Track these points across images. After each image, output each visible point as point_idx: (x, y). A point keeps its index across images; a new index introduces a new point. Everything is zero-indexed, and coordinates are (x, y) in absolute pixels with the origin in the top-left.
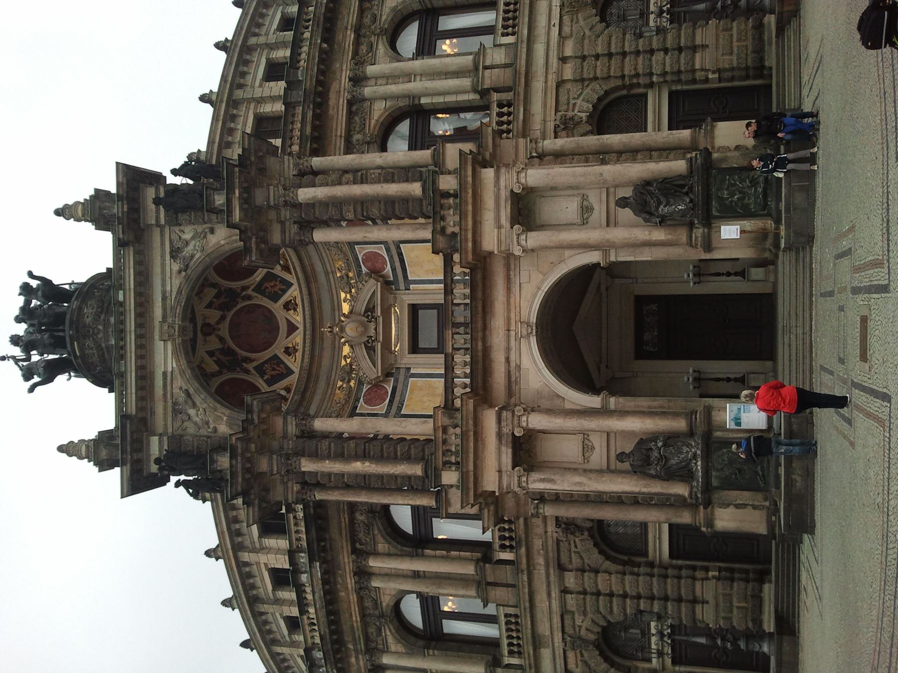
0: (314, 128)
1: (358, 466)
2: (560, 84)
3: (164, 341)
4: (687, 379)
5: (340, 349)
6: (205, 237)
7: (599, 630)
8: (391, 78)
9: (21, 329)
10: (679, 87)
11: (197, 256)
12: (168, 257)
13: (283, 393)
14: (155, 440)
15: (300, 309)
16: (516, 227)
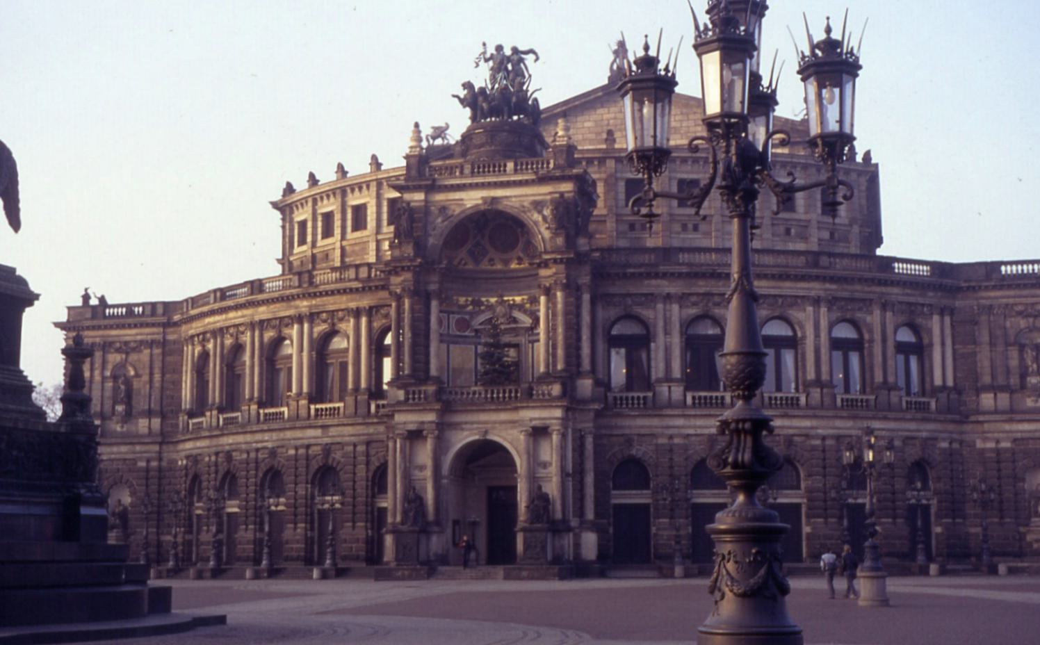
0: (633, 274)
4: (473, 517)
5: (493, 297)
7: (335, 465)
9: (508, 52)
10: (652, 510)
12: (532, 198)
13: (463, 262)
14: (419, 197)
15: (517, 266)
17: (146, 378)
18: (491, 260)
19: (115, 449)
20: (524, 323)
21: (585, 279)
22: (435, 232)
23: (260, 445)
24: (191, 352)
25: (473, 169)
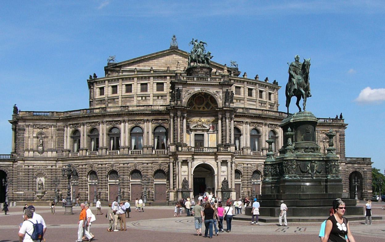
1: (179, 130)
2: (243, 164)
3: (201, 89)
6: (220, 98)
7: (139, 169)
8: (246, 129)
11: (217, 96)
15: (203, 110)
16: (222, 161)
17: (50, 138)
18: (195, 107)
19: (39, 162)
20: (206, 128)
21: (233, 116)
22: (185, 98)
23: (107, 162)
24: (69, 131)
25: (197, 79)
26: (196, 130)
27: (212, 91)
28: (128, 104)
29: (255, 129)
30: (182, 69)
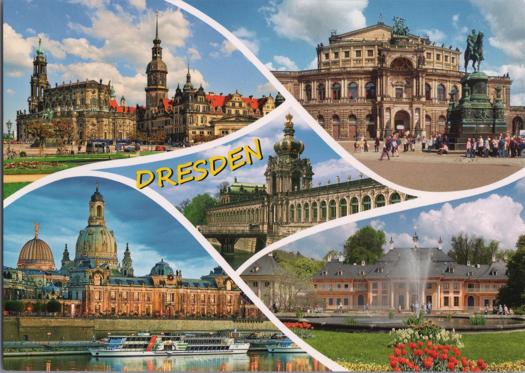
26: (396, 86)
27: (409, 56)
28: (347, 66)
29: (442, 85)
30: (387, 40)
